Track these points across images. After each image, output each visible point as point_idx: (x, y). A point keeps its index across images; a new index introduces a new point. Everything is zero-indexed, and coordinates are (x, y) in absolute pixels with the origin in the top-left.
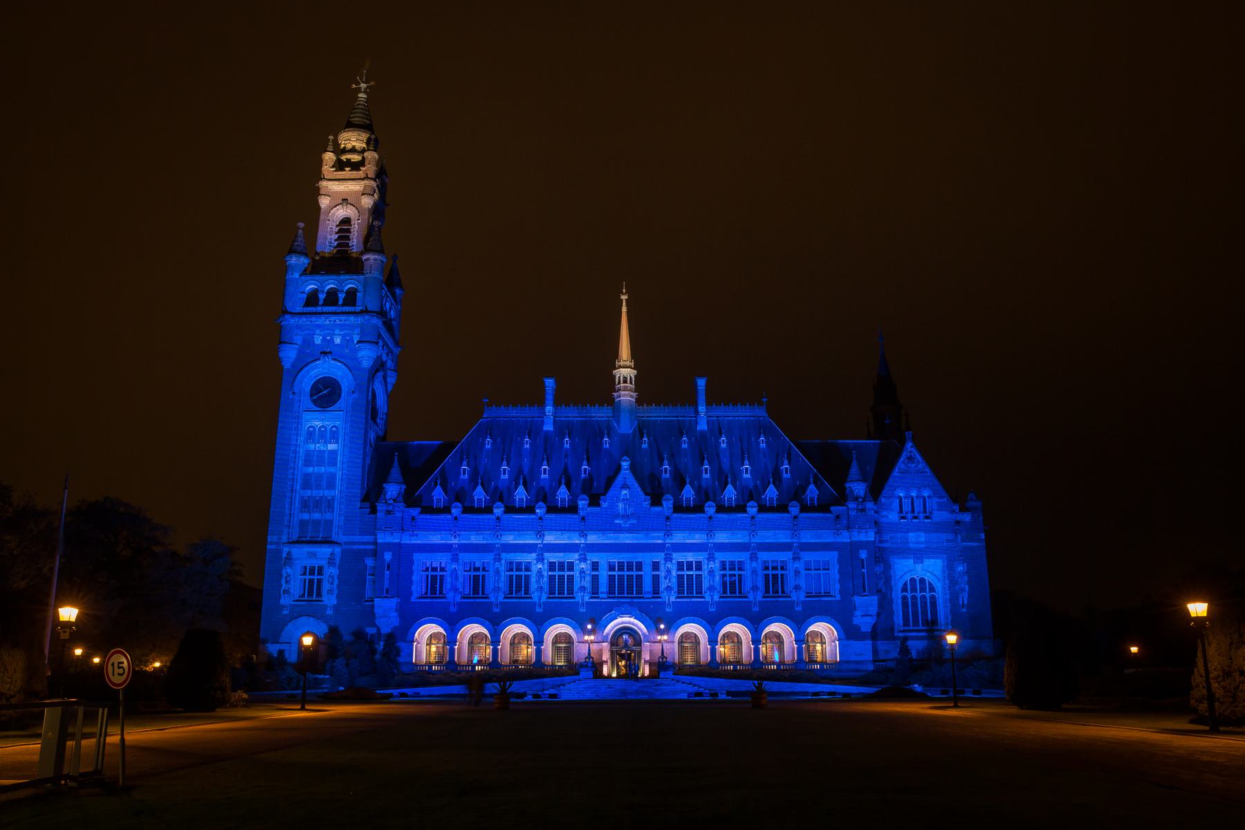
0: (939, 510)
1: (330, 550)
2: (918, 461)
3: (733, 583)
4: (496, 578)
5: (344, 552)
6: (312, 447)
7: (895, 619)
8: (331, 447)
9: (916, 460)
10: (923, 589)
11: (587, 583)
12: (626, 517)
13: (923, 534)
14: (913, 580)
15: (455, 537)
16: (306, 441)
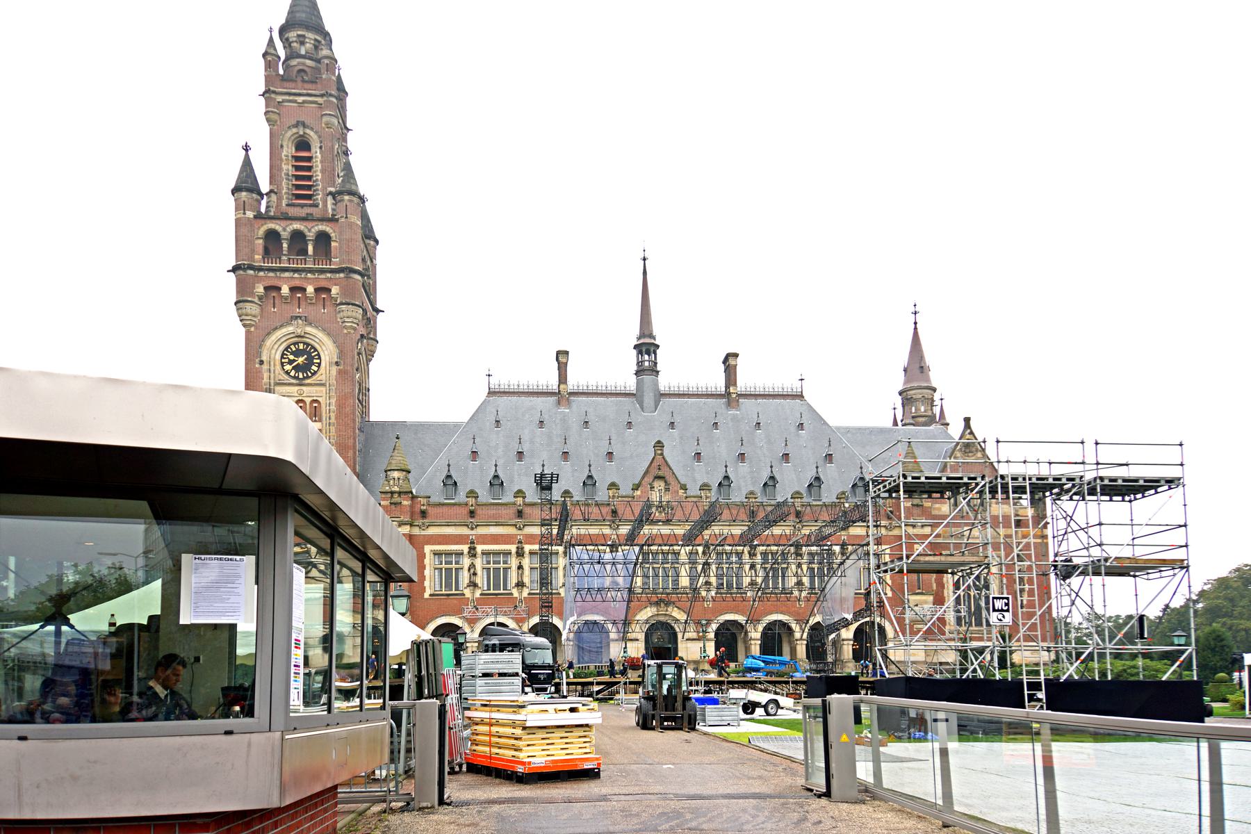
2: (977, 450)
4: (520, 572)
9: (974, 449)
15: (472, 529)
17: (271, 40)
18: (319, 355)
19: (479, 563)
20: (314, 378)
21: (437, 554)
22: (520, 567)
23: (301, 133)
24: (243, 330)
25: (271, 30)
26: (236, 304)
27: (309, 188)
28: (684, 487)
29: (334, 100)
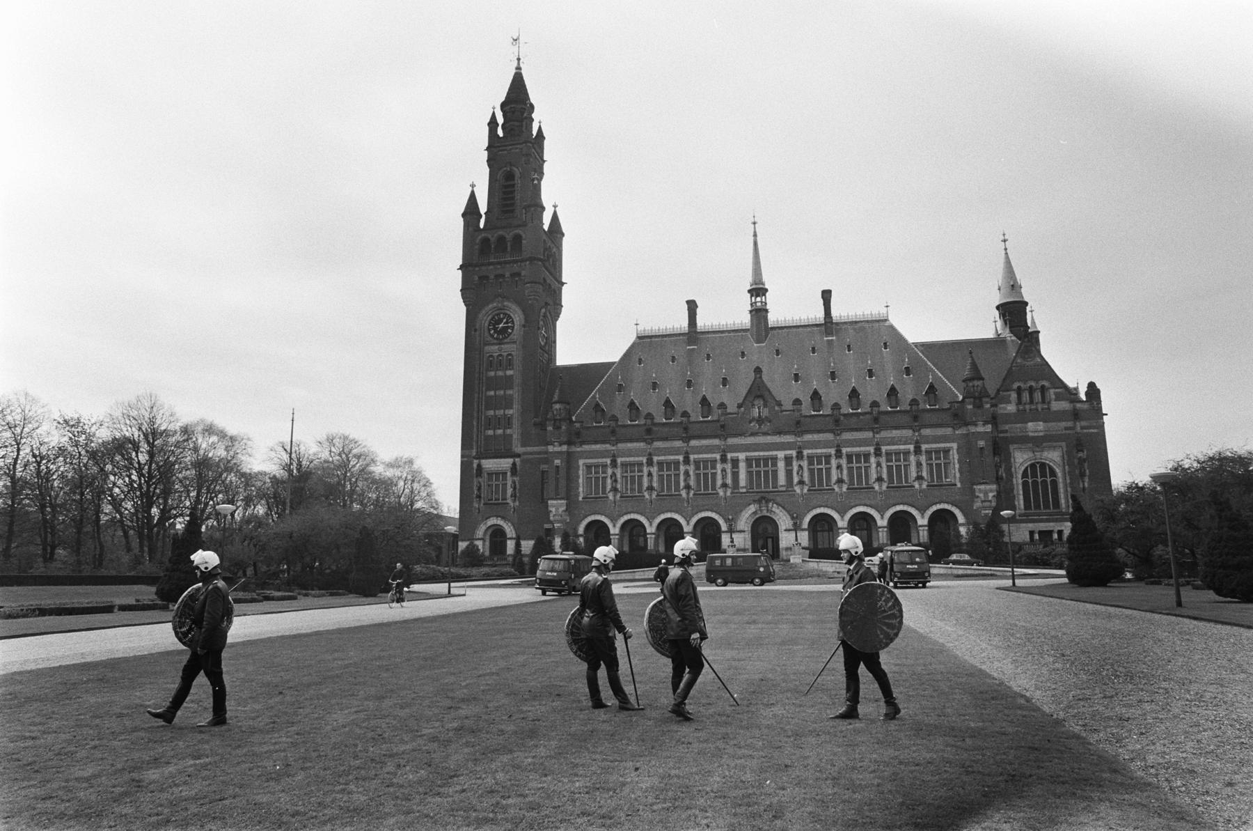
0: (1056, 400)
1: (511, 460)
3: (859, 476)
5: (522, 461)
6: (492, 374)
7: (1016, 503)
8: (509, 373)
11: (729, 481)
12: (760, 420)
13: (1041, 423)
14: (1033, 466)
16: (487, 370)
17: (494, 113)
19: (619, 472)
21: (588, 467)
22: (650, 474)
24: (465, 308)
25: (494, 108)
26: (461, 290)
28: (779, 404)
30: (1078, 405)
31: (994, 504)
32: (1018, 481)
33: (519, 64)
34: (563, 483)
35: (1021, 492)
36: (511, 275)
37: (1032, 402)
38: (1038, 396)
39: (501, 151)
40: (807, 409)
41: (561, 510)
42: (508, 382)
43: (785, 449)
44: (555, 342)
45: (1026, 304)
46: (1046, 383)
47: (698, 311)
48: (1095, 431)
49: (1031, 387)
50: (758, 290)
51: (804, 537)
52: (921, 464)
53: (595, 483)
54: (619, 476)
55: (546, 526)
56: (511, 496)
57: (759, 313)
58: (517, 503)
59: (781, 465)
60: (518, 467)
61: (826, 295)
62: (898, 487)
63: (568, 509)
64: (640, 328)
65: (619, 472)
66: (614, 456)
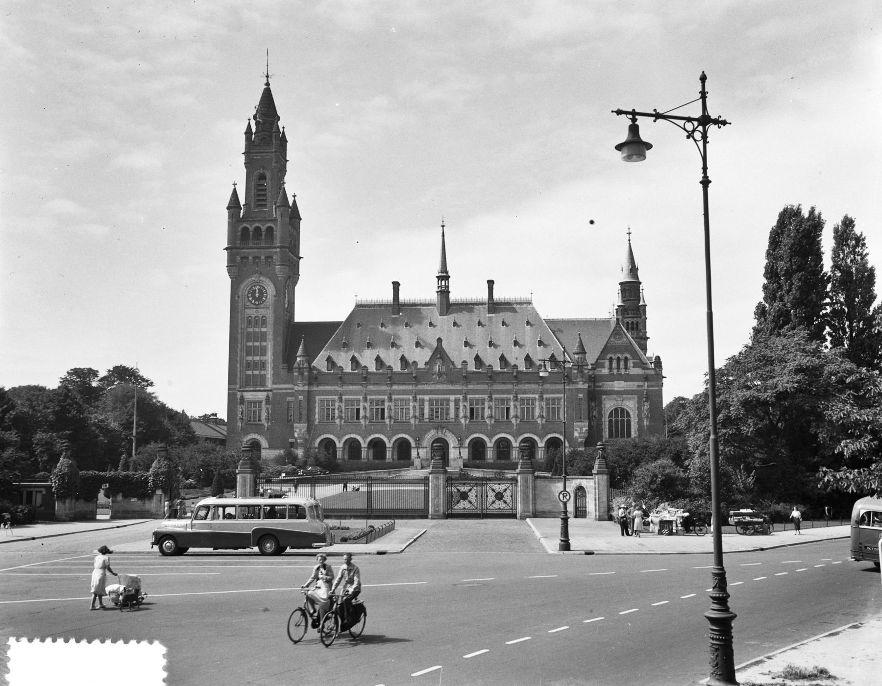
0: (633, 367)
1: (265, 393)
5: (274, 394)
6: (251, 330)
7: (603, 434)
8: (264, 330)
10: (622, 416)
11: (417, 414)
13: (623, 382)
14: (616, 409)
16: (247, 327)
17: (249, 124)
18: (266, 291)
20: (265, 303)
21: (322, 401)
23: (262, 172)
24: (230, 280)
25: (249, 120)
27: (265, 200)
28: (453, 363)
29: (278, 153)
30: (648, 372)
31: (586, 435)
32: (606, 420)
33: (268, 80)
34: (304, 412)
35: (607, 427)
36: (265, 258)
37: (618, 368)
38: (622, 364)
39: (256, 156)
40: (472, 367)
41: (303, 431)
42: (263, 337)
43: (456, 394)
44: (294, 303)
45: (641, 283)
46: (629, 356)
47: (400, 288)
48: (656, 388)
49: (618, 358)
50: (444, 276)
51: (465, 453)
52: (542, 408)
53: (329, 416)
54: (343, 408)
55: (290, 440)
56: (266, 419)
57: (444, 293)
58: (270, 424)
59: (452, 405)
60: (270, 399)
61: (491, 283)
62: (527, 422)
63: (309, 430)
64: (359, 299)
65: (343, 406)
66: (341, 395)
